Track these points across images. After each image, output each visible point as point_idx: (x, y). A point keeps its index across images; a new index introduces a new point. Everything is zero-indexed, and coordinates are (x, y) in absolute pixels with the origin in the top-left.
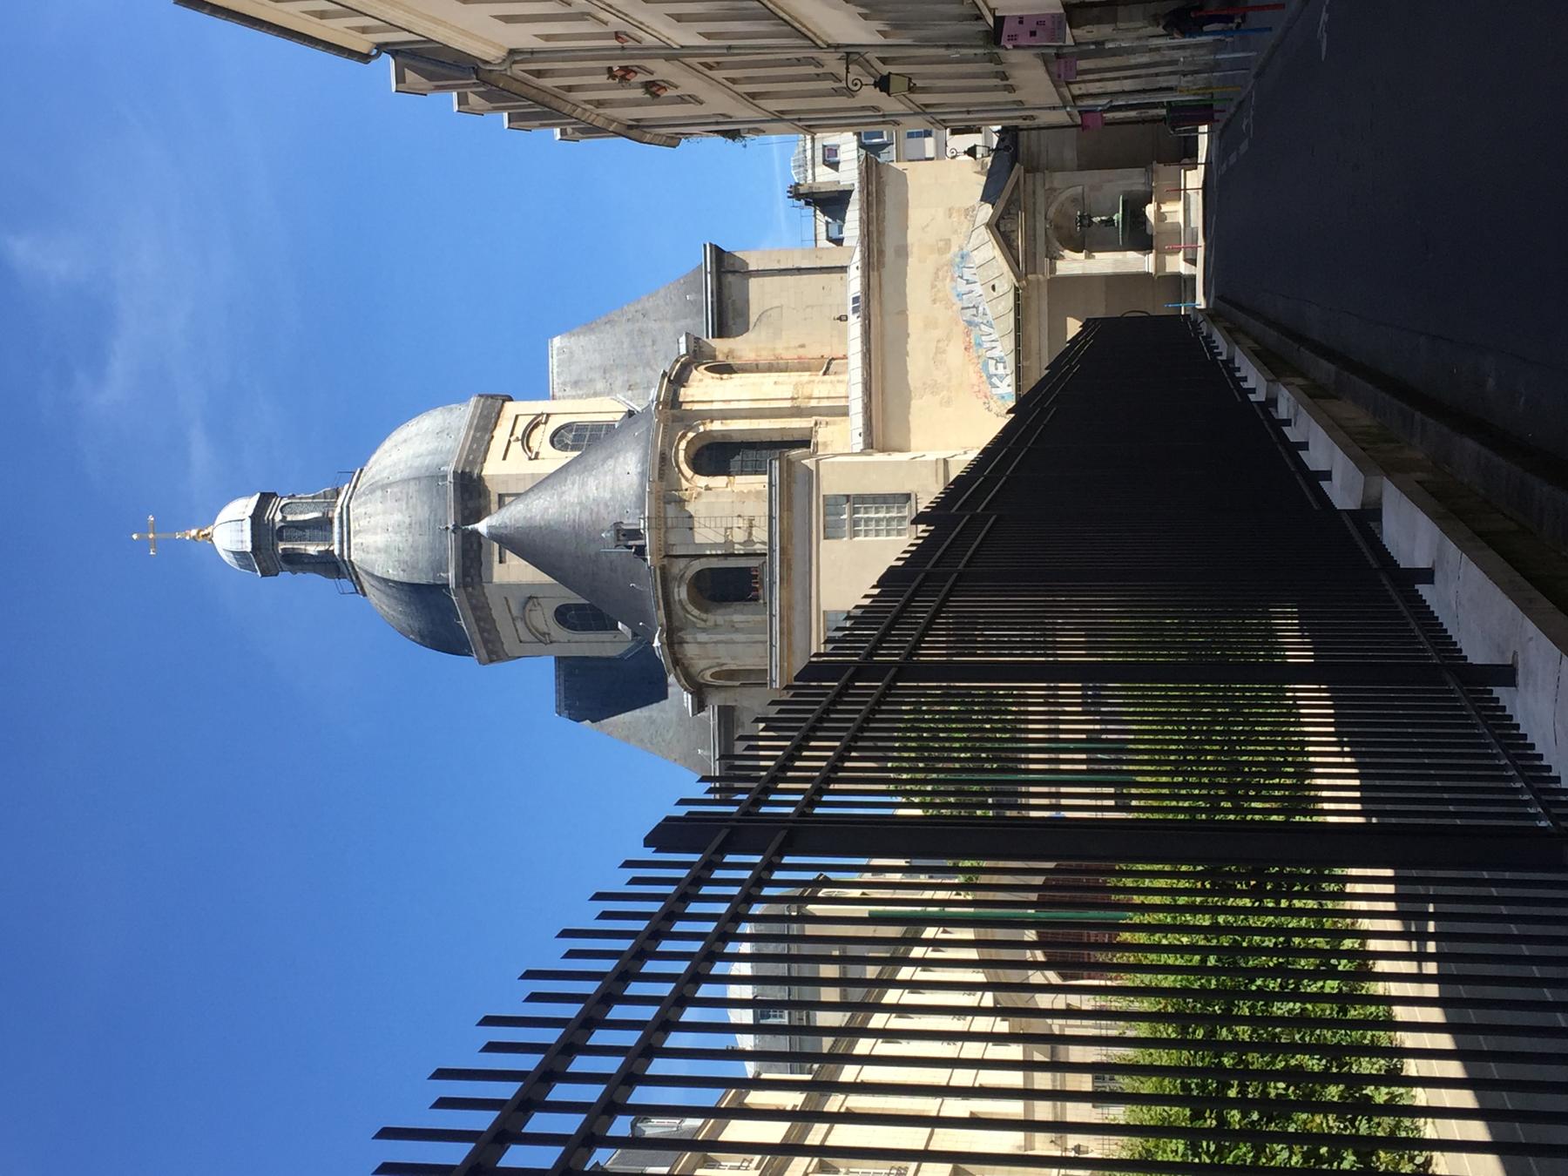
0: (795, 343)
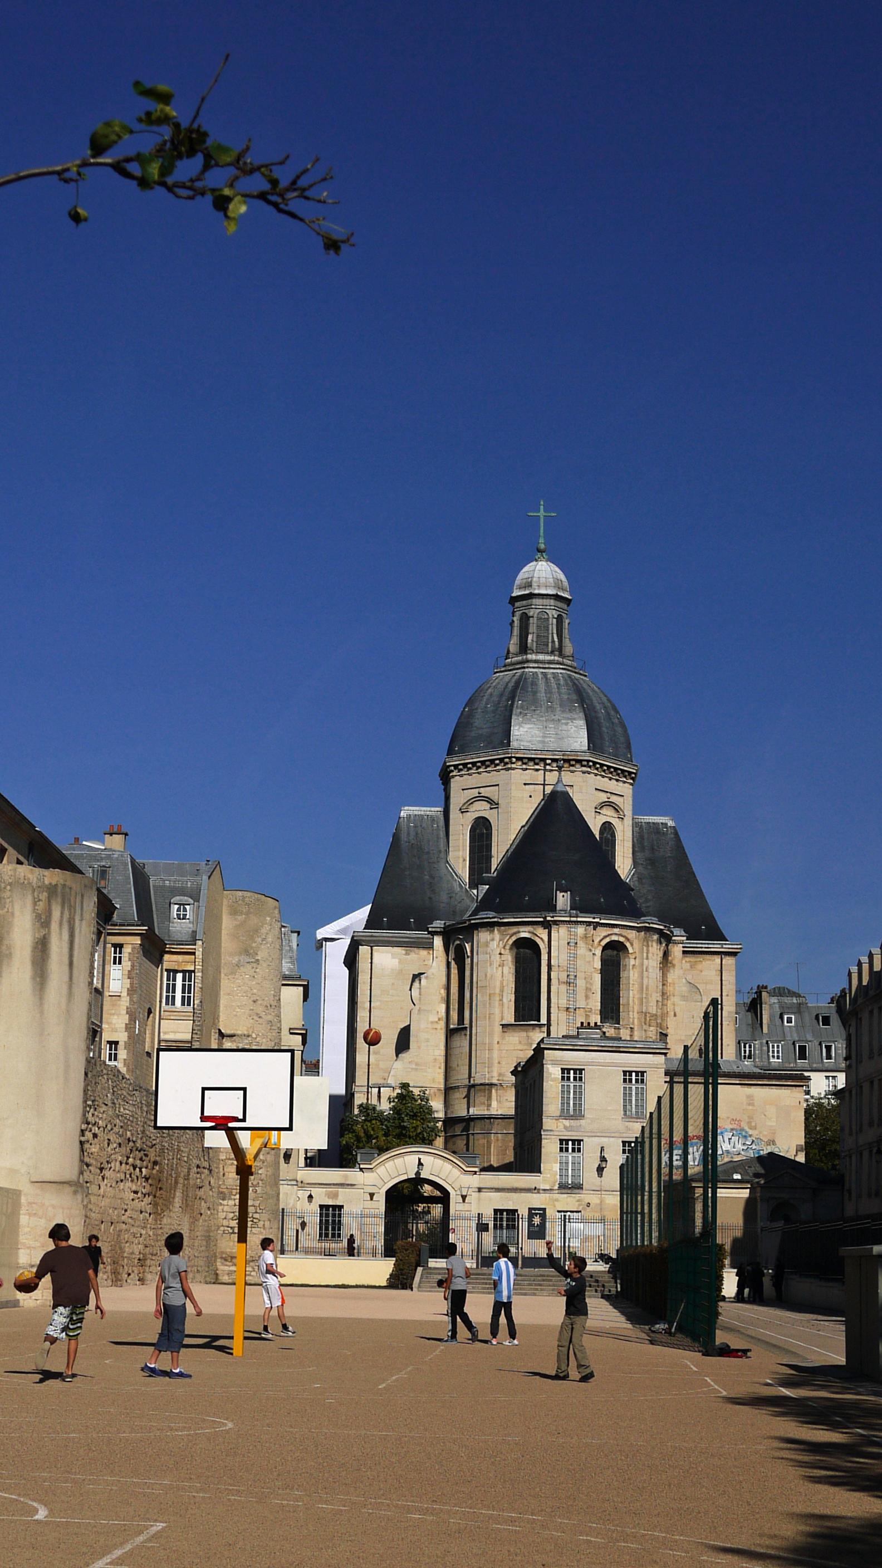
0: (677, 1010)
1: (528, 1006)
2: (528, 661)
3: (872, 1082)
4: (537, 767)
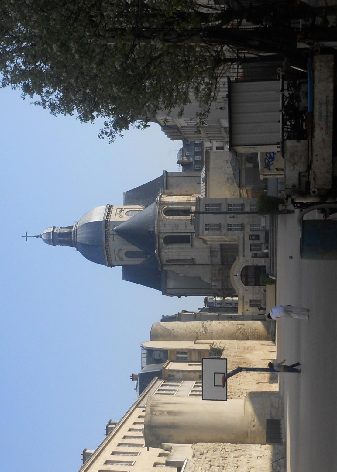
1: (185, 239)
2: (74, 240)
3: (207, 134)
4: (108, 237)
